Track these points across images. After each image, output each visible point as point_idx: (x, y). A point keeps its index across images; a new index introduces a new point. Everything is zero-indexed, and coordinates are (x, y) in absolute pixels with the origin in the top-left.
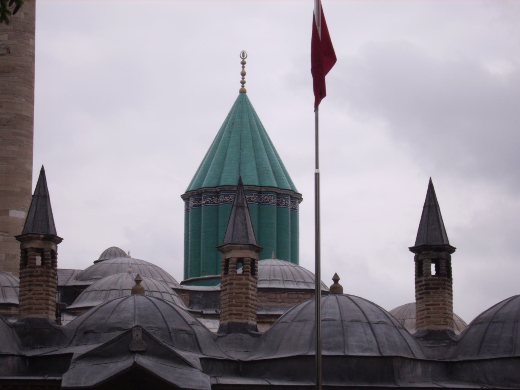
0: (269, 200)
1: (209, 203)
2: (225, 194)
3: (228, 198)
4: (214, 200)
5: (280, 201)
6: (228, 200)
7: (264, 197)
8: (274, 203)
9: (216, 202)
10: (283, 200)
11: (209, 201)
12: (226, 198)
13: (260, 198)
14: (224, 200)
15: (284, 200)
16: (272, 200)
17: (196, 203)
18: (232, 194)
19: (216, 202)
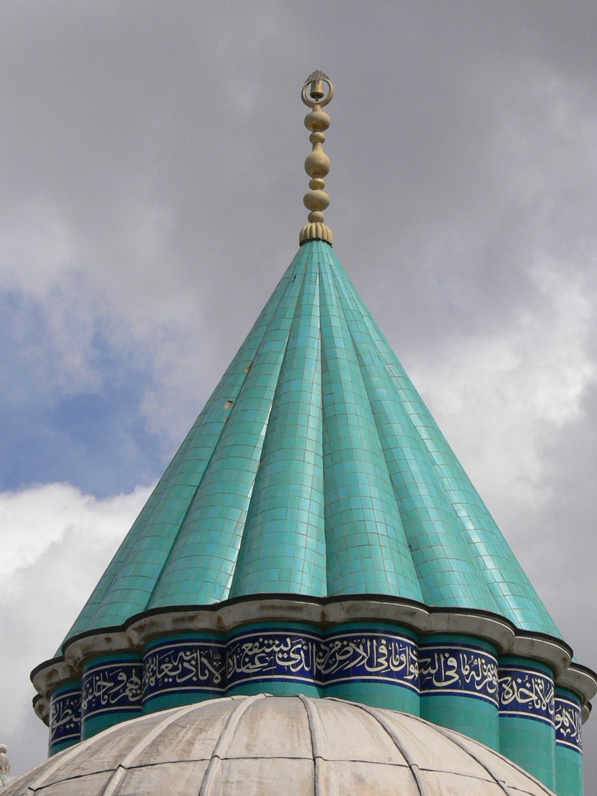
0: (365, 661)
1: (104, 703)
2: (161, 653)
3: (175, 669)
4: (125, 688)
5: (434, 668)
6: (174, 677)
7: (343, 646)
8: (401, 675)
9: (134, 696)
10: (446, 659)
11: (104, 694)
12: (166, 667)
13: (328, 655)
14: (157, 679)
15: (452, 662)
16: (382, 660)
17: (67, 719)
18: (191, 649)
19: (134, 696)
